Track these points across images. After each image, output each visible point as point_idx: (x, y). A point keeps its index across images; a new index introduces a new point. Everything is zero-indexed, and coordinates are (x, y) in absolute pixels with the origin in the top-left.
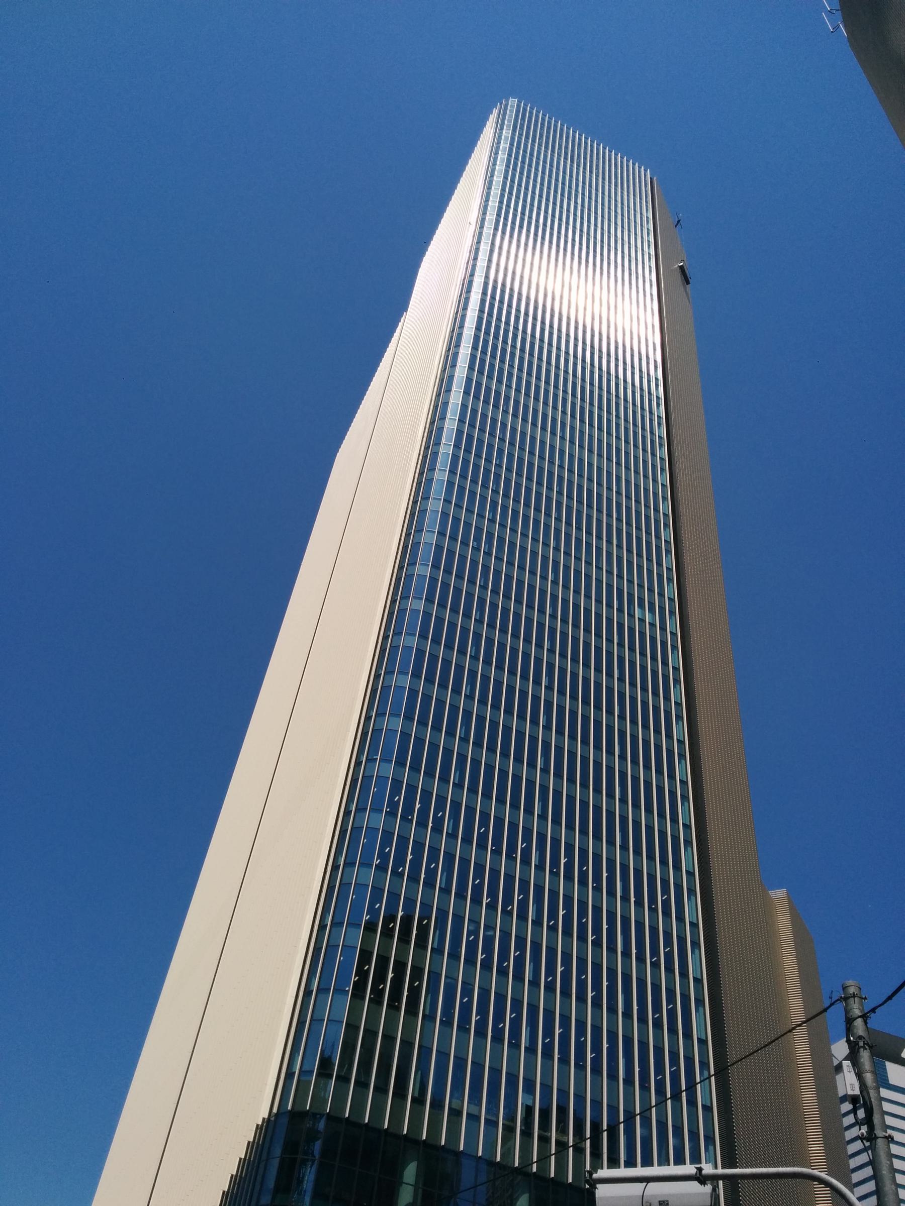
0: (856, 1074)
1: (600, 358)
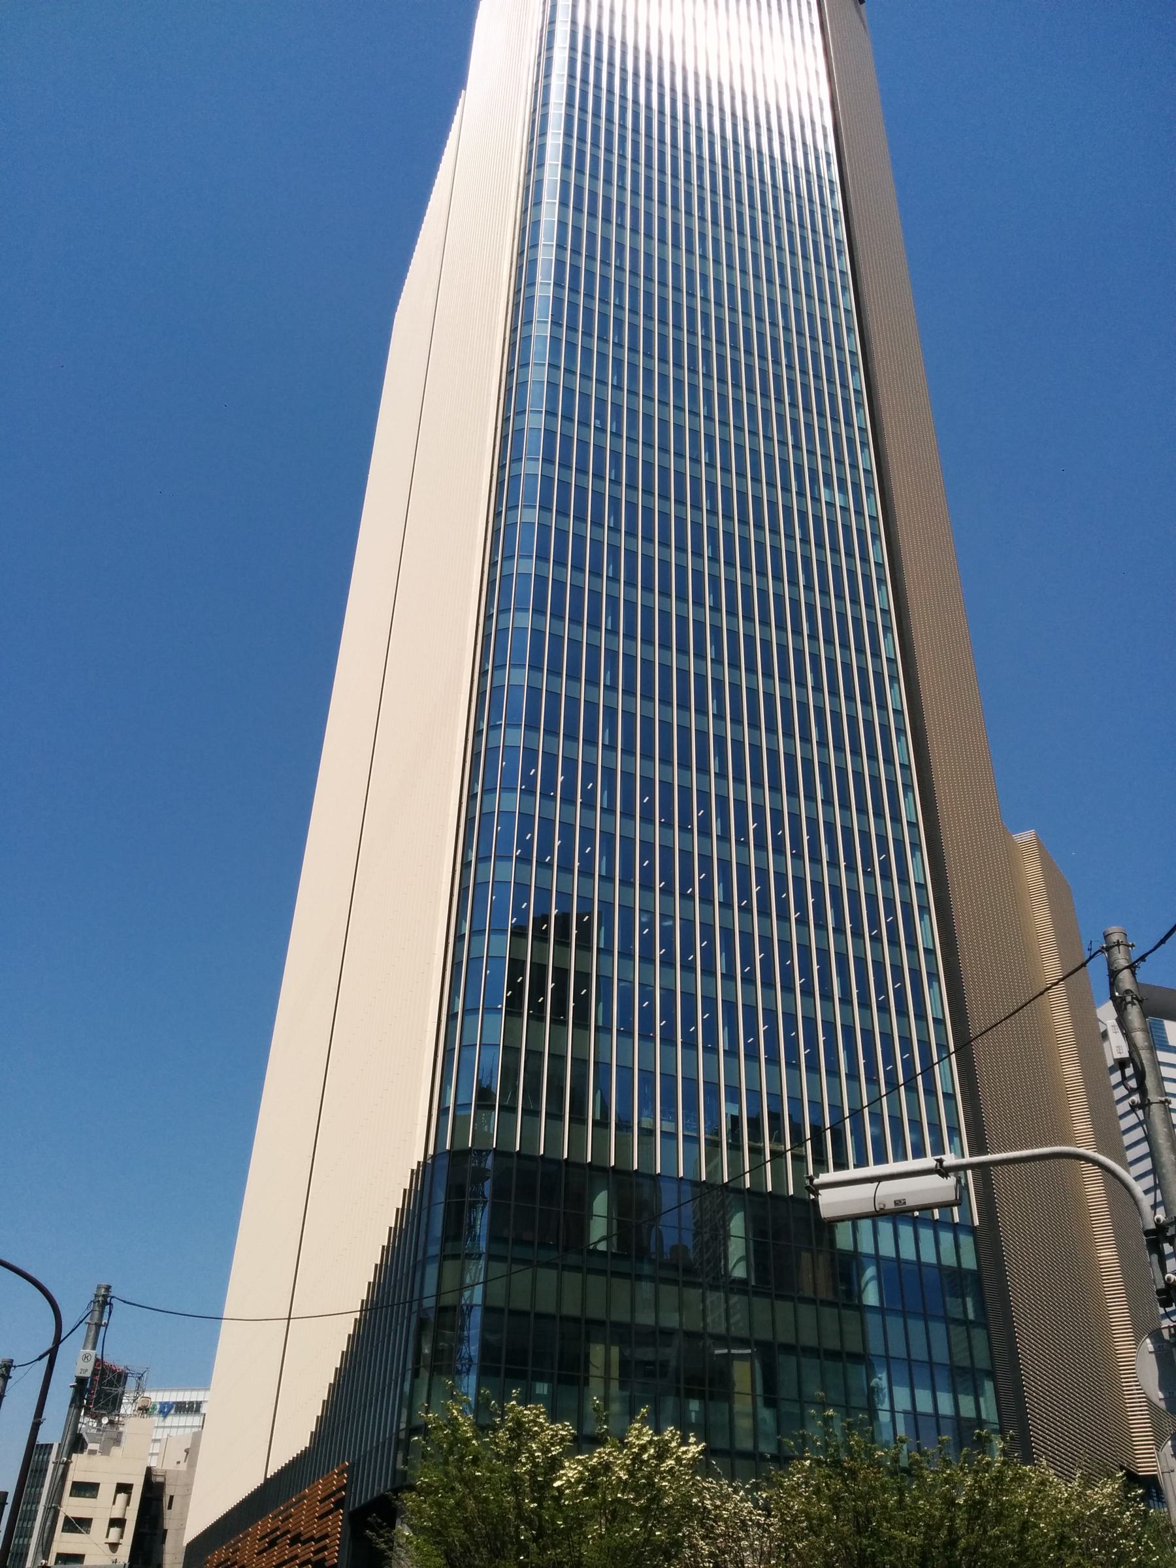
0: (1123, 1034)
1: (746, 130)
